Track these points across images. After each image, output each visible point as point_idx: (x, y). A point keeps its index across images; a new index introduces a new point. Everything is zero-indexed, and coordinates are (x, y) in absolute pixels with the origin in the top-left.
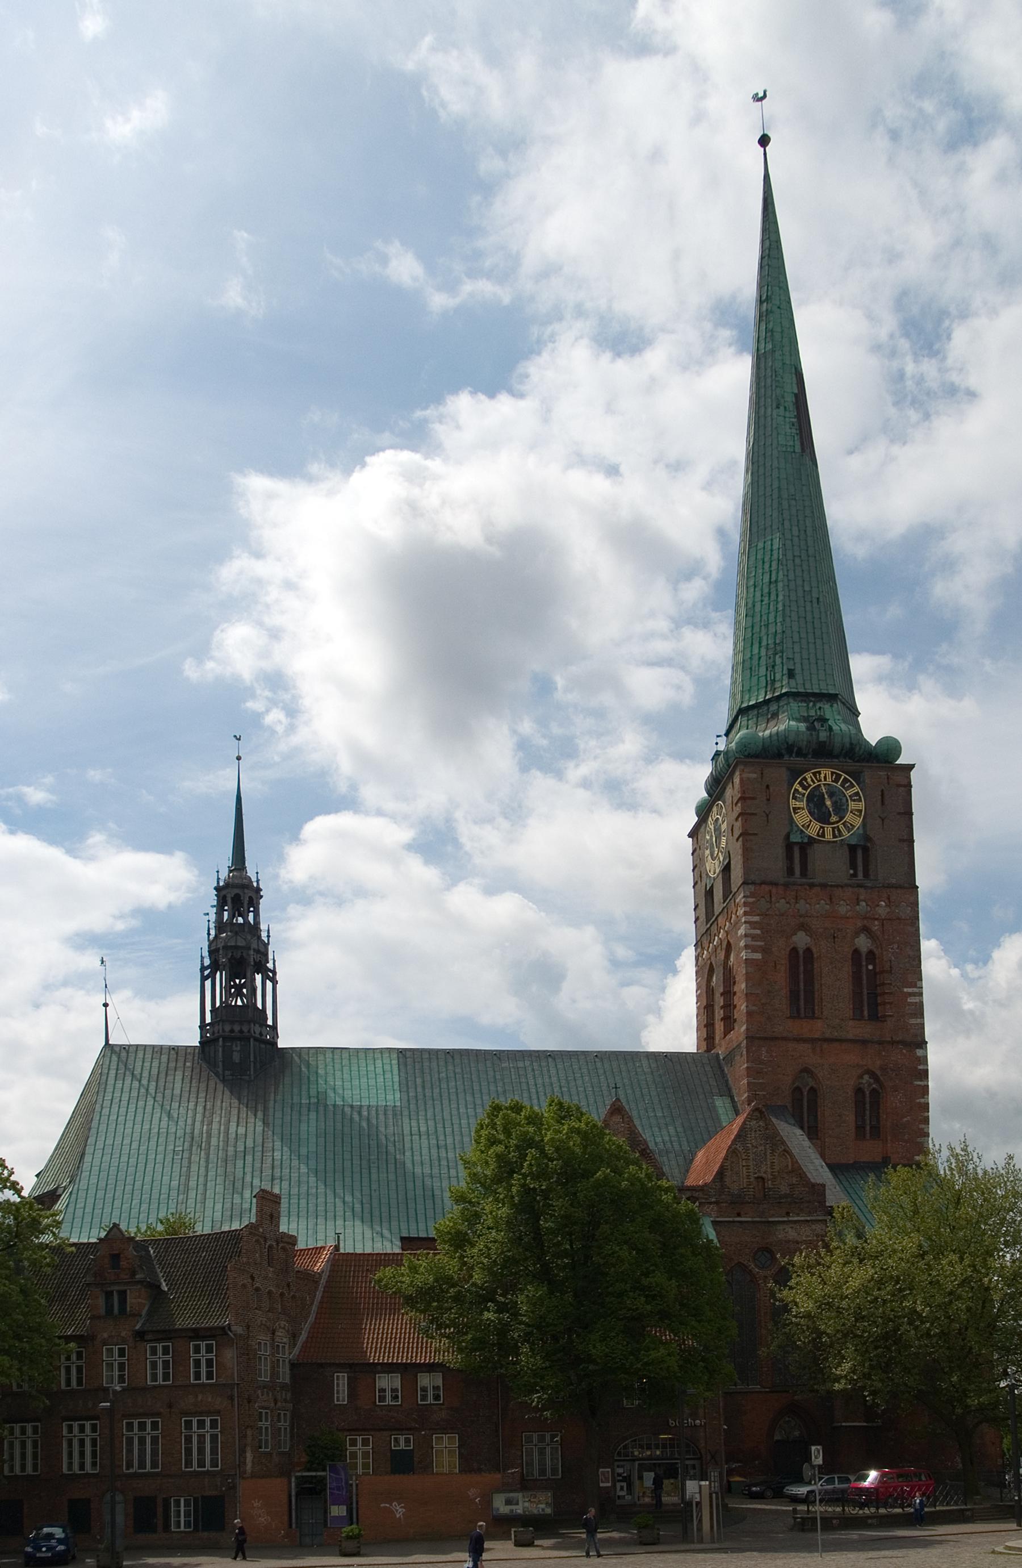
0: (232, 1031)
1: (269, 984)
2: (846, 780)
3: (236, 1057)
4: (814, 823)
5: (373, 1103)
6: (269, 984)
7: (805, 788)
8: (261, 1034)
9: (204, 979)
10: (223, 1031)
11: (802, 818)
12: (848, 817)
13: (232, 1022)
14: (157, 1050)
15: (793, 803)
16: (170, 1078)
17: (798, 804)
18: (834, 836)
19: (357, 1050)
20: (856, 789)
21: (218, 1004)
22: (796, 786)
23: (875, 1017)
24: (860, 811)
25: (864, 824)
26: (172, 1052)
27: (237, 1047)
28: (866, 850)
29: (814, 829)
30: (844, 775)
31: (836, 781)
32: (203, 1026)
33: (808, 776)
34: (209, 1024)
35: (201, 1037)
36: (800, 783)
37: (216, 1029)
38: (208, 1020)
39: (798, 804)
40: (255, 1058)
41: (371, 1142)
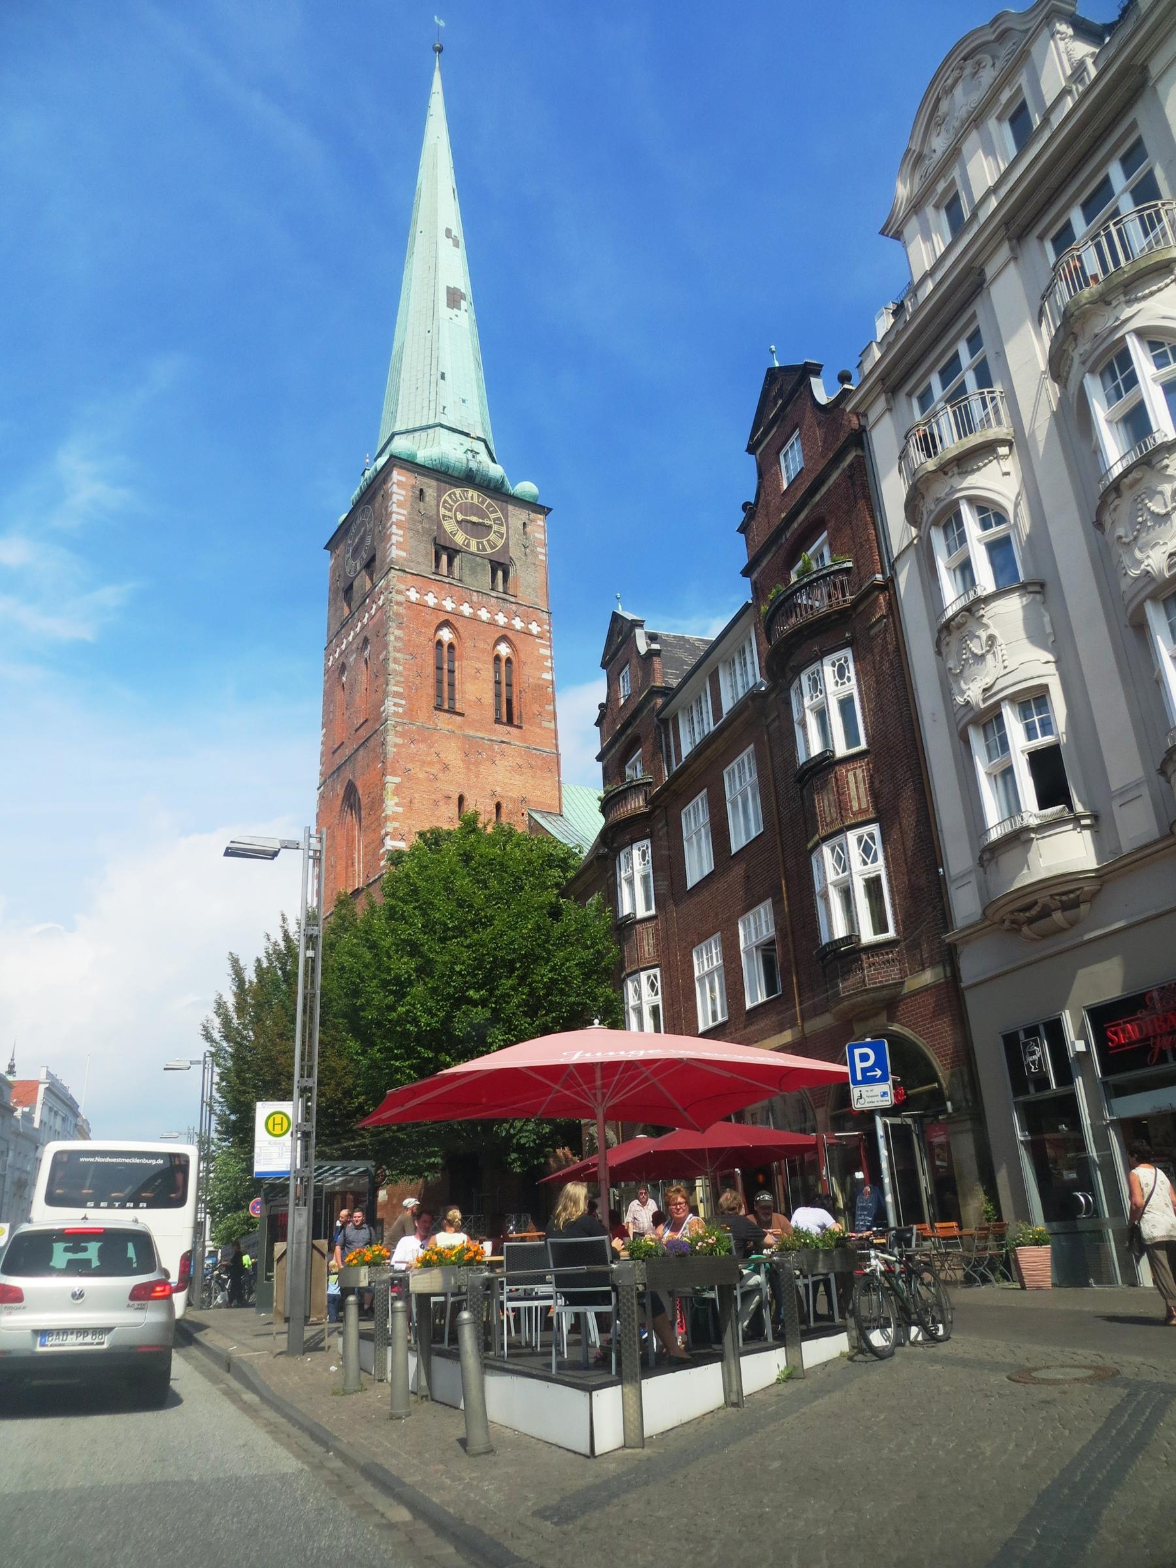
2: (489, 506)
4: (460, 533)
7: (455, 502)
11: (449, 526)
12: (492, 537)
15: (442, 511)
17: (447, 513)
18: (478, 549)
20: (499, 514)
22: (446, 497)
23: (510, 721)
24: (502, 534)
25: (506, 546)
29: (460, 539)
30: (489, 500)
31: (483, 502)
33: (458, 491)
36: (450, 496)
39: (447, 513)
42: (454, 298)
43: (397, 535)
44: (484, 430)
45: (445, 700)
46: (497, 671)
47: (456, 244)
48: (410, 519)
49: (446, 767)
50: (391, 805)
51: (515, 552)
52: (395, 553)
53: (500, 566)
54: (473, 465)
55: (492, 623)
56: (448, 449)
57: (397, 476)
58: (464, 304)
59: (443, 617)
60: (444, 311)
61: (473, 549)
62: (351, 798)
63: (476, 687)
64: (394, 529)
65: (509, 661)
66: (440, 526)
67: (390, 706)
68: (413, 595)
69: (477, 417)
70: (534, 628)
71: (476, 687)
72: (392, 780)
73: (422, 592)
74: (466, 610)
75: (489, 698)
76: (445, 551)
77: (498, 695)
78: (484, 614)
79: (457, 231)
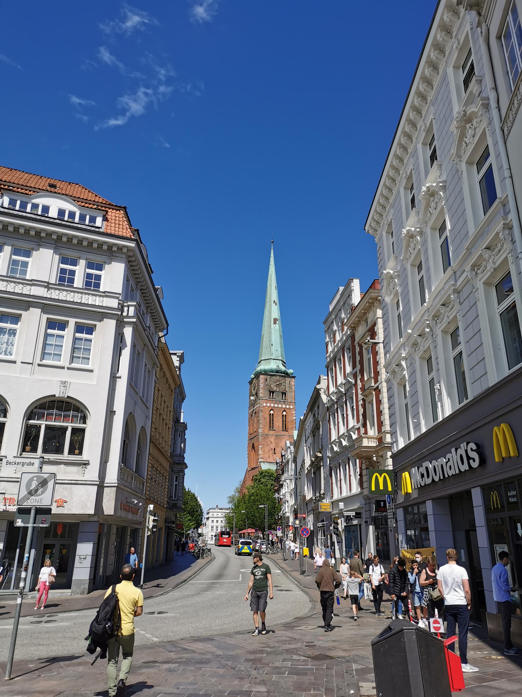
11: (272, 386)
28: (285, 394)
29: (275, 389)
42: (275, 320)
43: (261, 391)
44: (282, 356)
45: (271, 426)
46: (283, 418)
47: (276, 305)
48: (264, 386)
49: (271, 442)
50: (260, 452)
51: (287, 389)
52: (261, 395)
53: (284, 394)
54: (278, 369)
55: (282, 408)
56: (273, 365)
57: (261, 376)
58: (277, 322)
59: (271, 408)
60: (273, 326)
61: (278, 390)
62: (253, 447)
63: (278, 423)
64: (261, 390)
65: (286, 416)
66: (270, 387)
67: (260, 430)
68: (265, 404)
69: (280, 353)
70: (291, 407)
71: (278, 423)
72: (260, 447)
73: (266, 403)
74: (276, 405)
75: (281, 425)
76: (272, 392)
77: (283, 424)
78: (280, 406)
79: (277, 301)
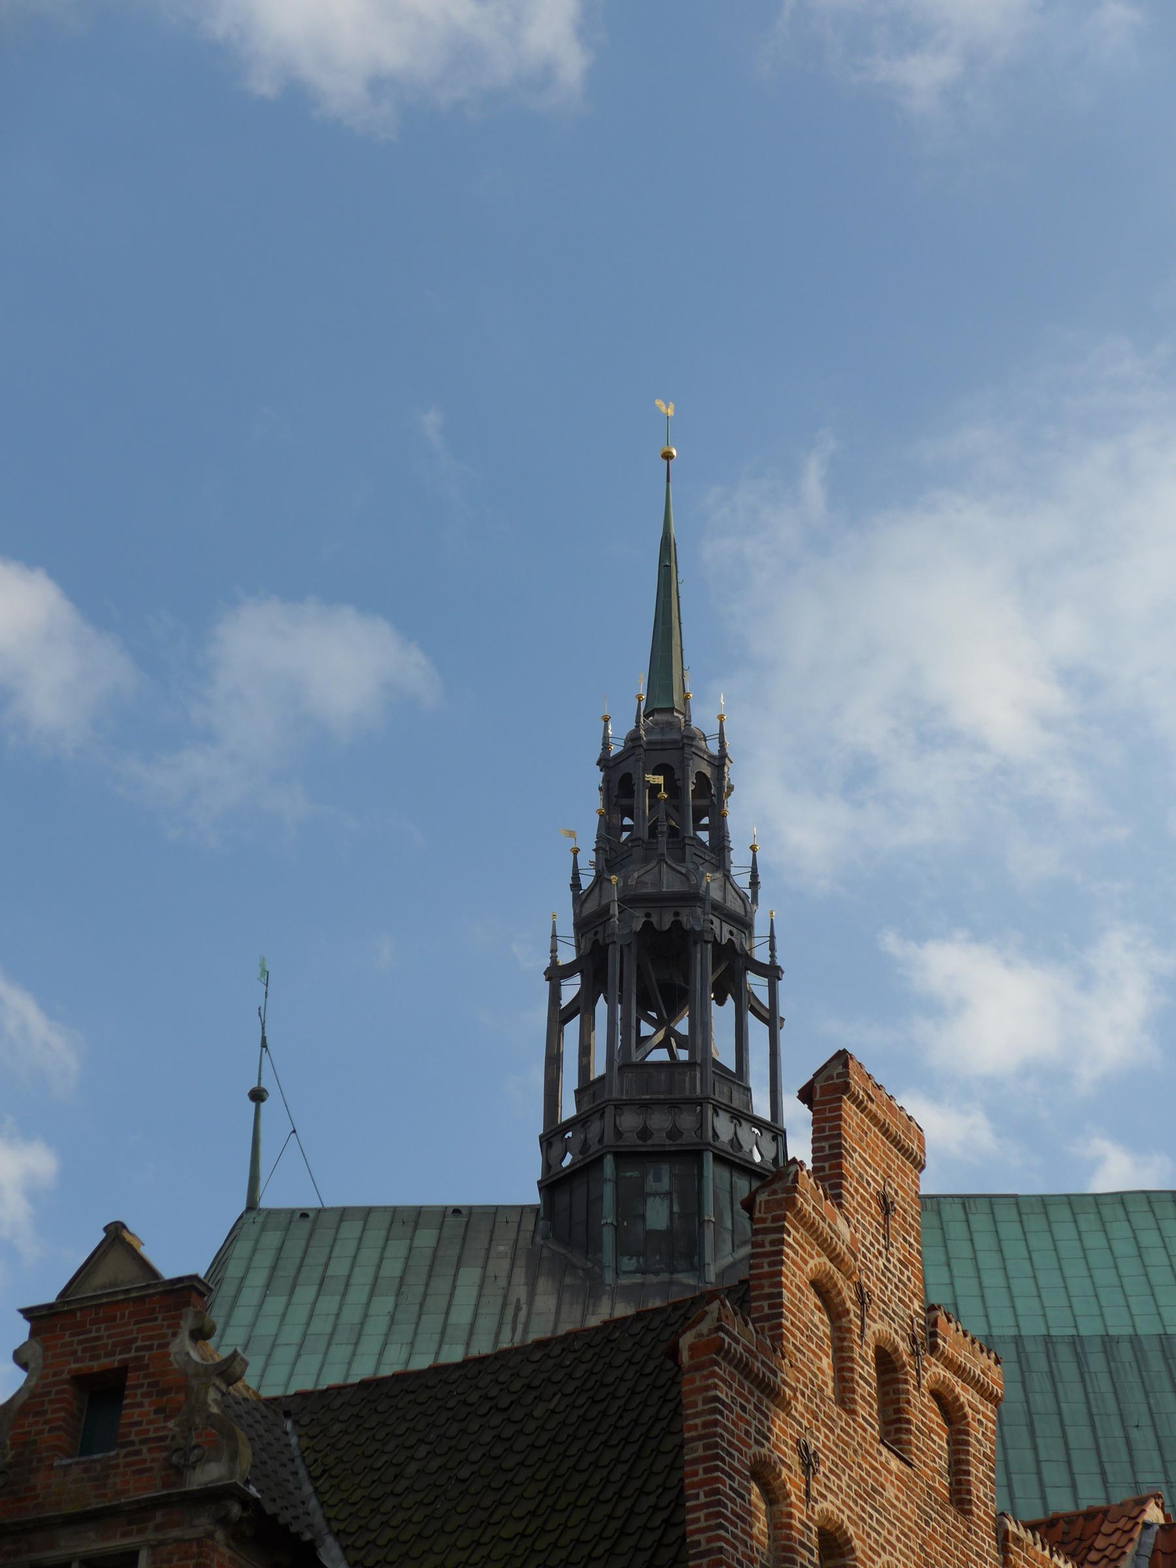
0: (645, 1133)
1: (757, 1030)
3: (657, 1215)
5: (1119, 1327)
6: (757, 1030)
8: (736, 1143)
9: (559, 1017)
10: (619, 1134)
13: (645, 1106)
14: (409, 1219)
16: (441, 1286)
19: (1044, 1202)
21: (599, 1068)
26: (450, 1220)
27: (662, 1179)
32: (552, 1136)
34: (570, 1124)
35: (547, 1166)
37: (595, 1128)
38: (568, 1109)
40: (719, 1214)
41: (1135, 1434)
